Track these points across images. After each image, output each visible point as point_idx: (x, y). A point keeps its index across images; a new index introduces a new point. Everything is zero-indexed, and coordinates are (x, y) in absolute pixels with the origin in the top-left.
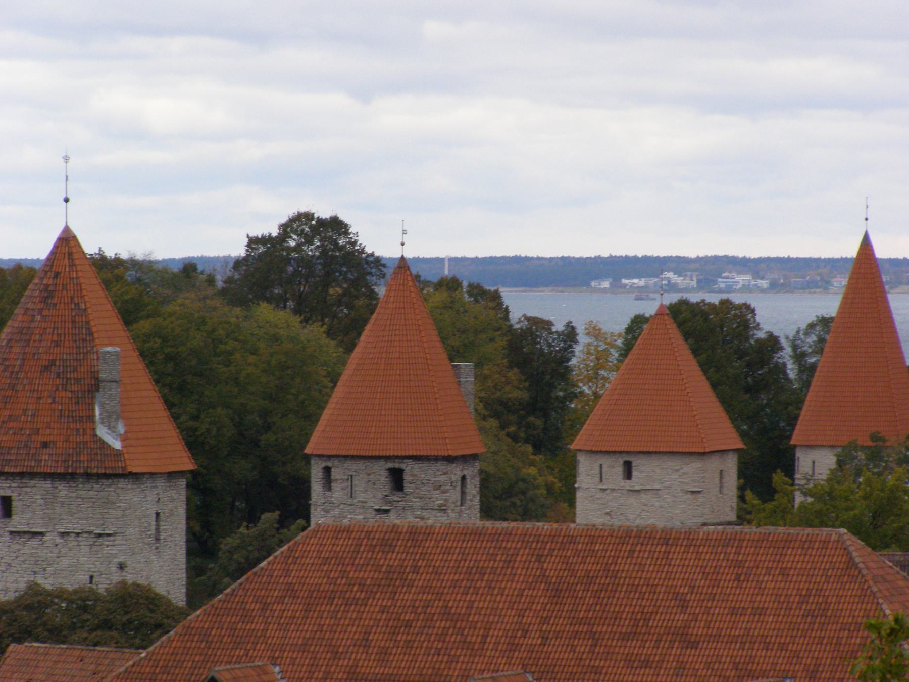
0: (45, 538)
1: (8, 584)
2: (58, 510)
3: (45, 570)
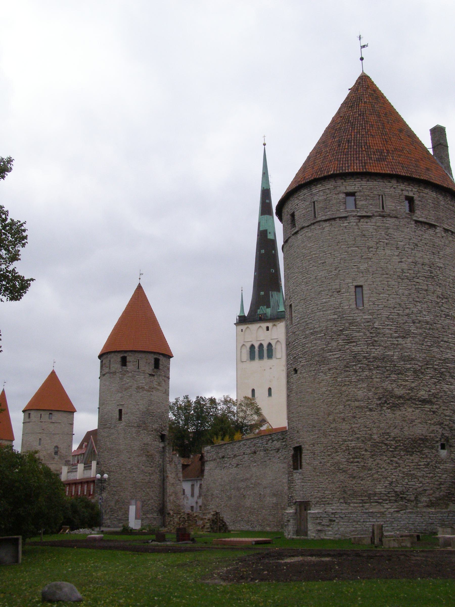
0: (437, 231)
1: (417, 259)
2: (441, 214)
3: (439, 253)
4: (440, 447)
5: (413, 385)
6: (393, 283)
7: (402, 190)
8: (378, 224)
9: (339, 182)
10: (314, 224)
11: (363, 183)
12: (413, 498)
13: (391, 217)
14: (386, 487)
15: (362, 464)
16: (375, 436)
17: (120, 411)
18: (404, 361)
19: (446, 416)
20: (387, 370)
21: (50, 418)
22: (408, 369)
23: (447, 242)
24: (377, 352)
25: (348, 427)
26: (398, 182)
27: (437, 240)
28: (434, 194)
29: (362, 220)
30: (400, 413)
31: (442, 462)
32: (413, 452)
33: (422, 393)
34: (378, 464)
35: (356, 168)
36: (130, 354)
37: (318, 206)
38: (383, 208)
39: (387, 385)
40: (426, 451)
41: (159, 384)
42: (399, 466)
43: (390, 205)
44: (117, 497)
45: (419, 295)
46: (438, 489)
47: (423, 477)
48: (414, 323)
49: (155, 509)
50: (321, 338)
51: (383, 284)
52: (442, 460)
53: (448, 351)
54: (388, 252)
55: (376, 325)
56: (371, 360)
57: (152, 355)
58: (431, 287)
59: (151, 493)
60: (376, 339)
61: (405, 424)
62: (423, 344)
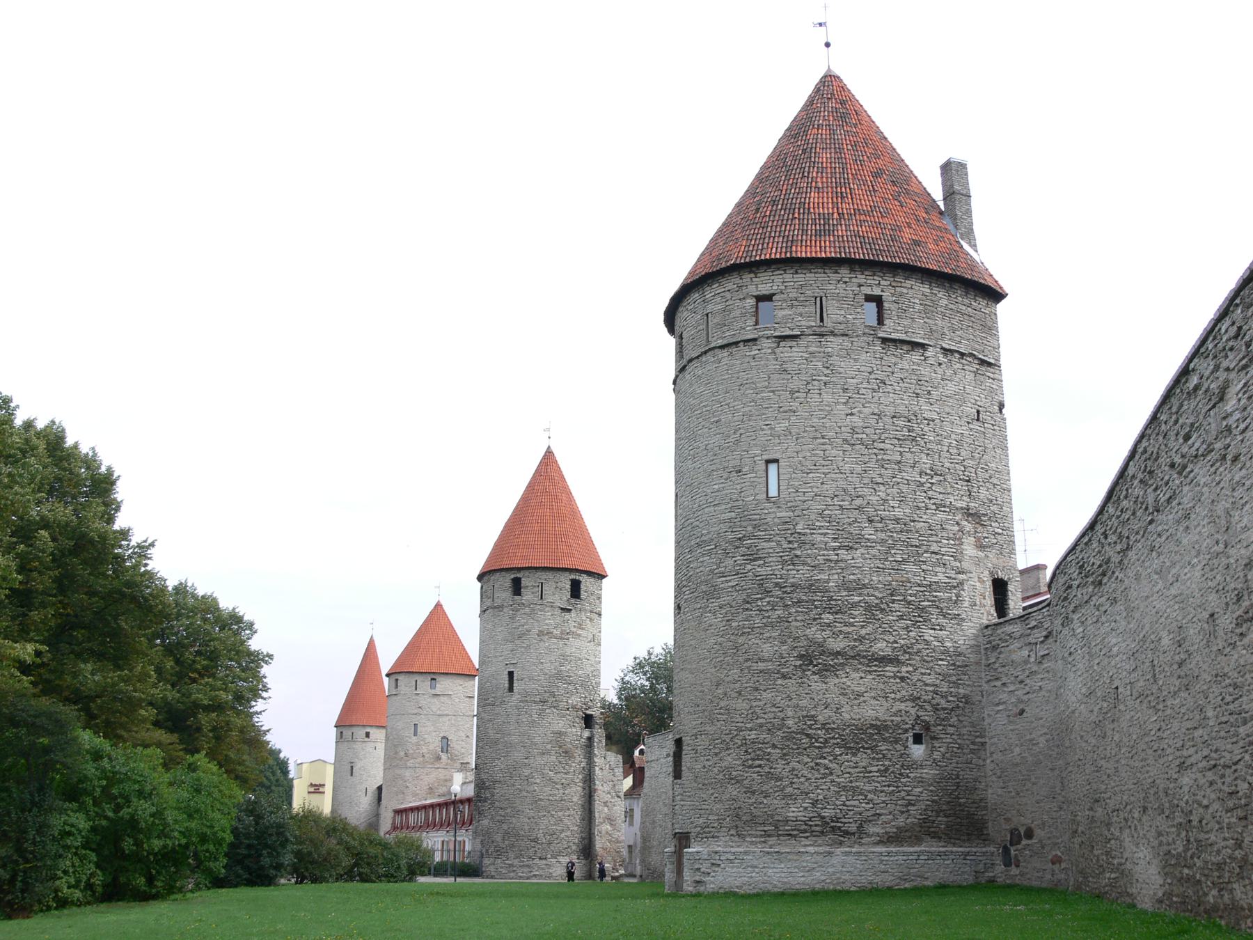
0: (927, 354)
2: (939, 322)
3: (929, 393)
4: (911, 739)
5: (863, 632)
6: (834, 452)
7: (860, 286)
8: (811, 349)
9: (747, 277)
10: (705, 352)
11: (788, 277)
12: (853, 828)
13: (835, 335)
14: (806, 808)
15: (767, 770)
16: (790, 722)
17: (511, 674)
18: (848, 589)
19: (926, 685)
20: (816, 607)
21: (433, 687)
22: (855, 605)
23: (949, 372)
24: (799, 575)
25: (745, 705)
26: (852, 270)
27: (926, 371)
28: (926, 289)
29: (782, 344)
30: (837, 681)
31: (915, 765)
32: (858, 750)
33: (881, 645)
34: (794, 769)
35: (774, 251)
36: (527, 573)
37: (714, 321)
38: (822, 320)
39: (813, 632)
40: (883, 747)
41: (580, 626)
42: (831, 774)
43: (834, 313)
44: (505, 827)
45: (883, 471)
46: (902, 812)
47: (875, 791)
48: (871, 522)
49: (574, 848)
50: (709, 553)
51: (815, 455)
52: (915, 763)
53: (938, 569)
54: (827, 398)
55: (799, 528)
56: (788, 589)
57: (567, 574)
58: (908, 456)
59: (566, 820)
60: (798, 553)
61: (844, 700)
62: (886, 559)
